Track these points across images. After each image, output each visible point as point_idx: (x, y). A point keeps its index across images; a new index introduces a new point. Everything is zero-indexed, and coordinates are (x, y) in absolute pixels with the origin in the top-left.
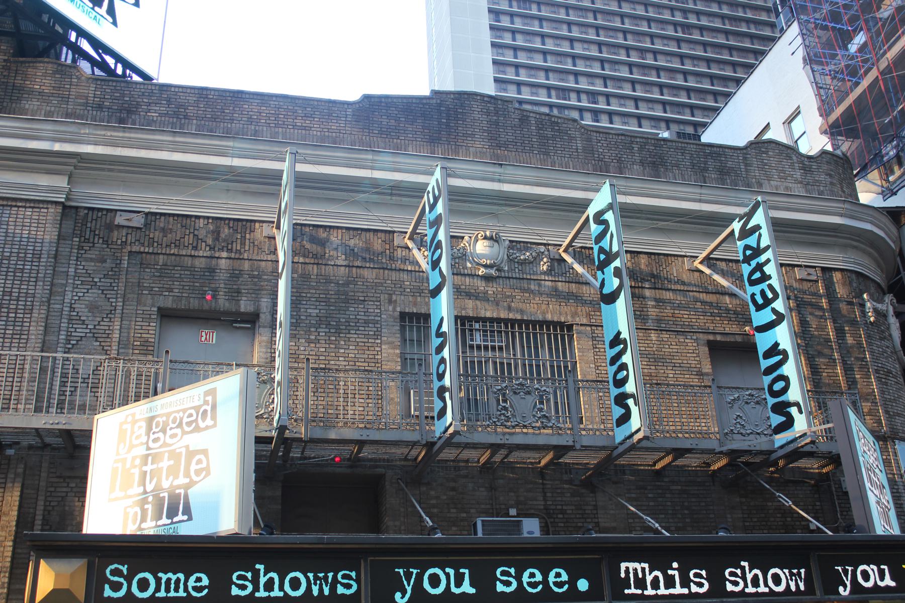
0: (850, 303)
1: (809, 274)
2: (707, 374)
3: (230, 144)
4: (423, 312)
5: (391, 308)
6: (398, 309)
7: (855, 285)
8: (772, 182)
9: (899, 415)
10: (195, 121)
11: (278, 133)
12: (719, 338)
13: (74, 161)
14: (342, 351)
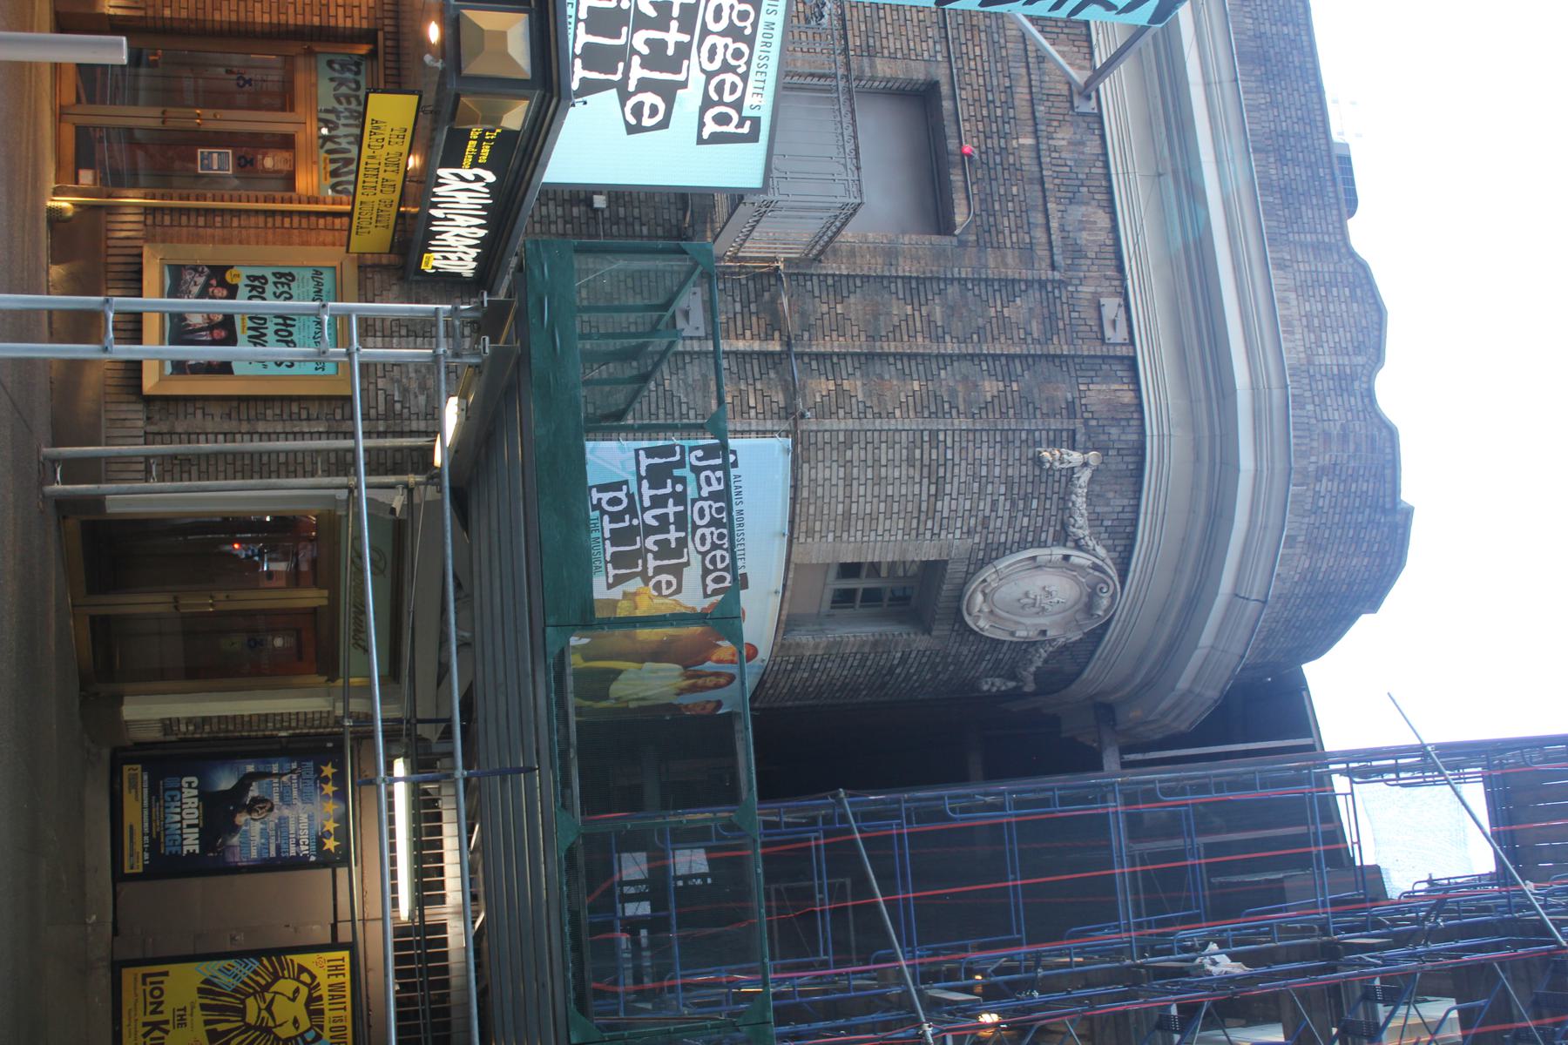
0: (1071, 409)
1: (1114, 322)
2: (872, 66)
7: (1114, 431)
8: (1293, 296)
9: (848, 482)
12: (947, 104)
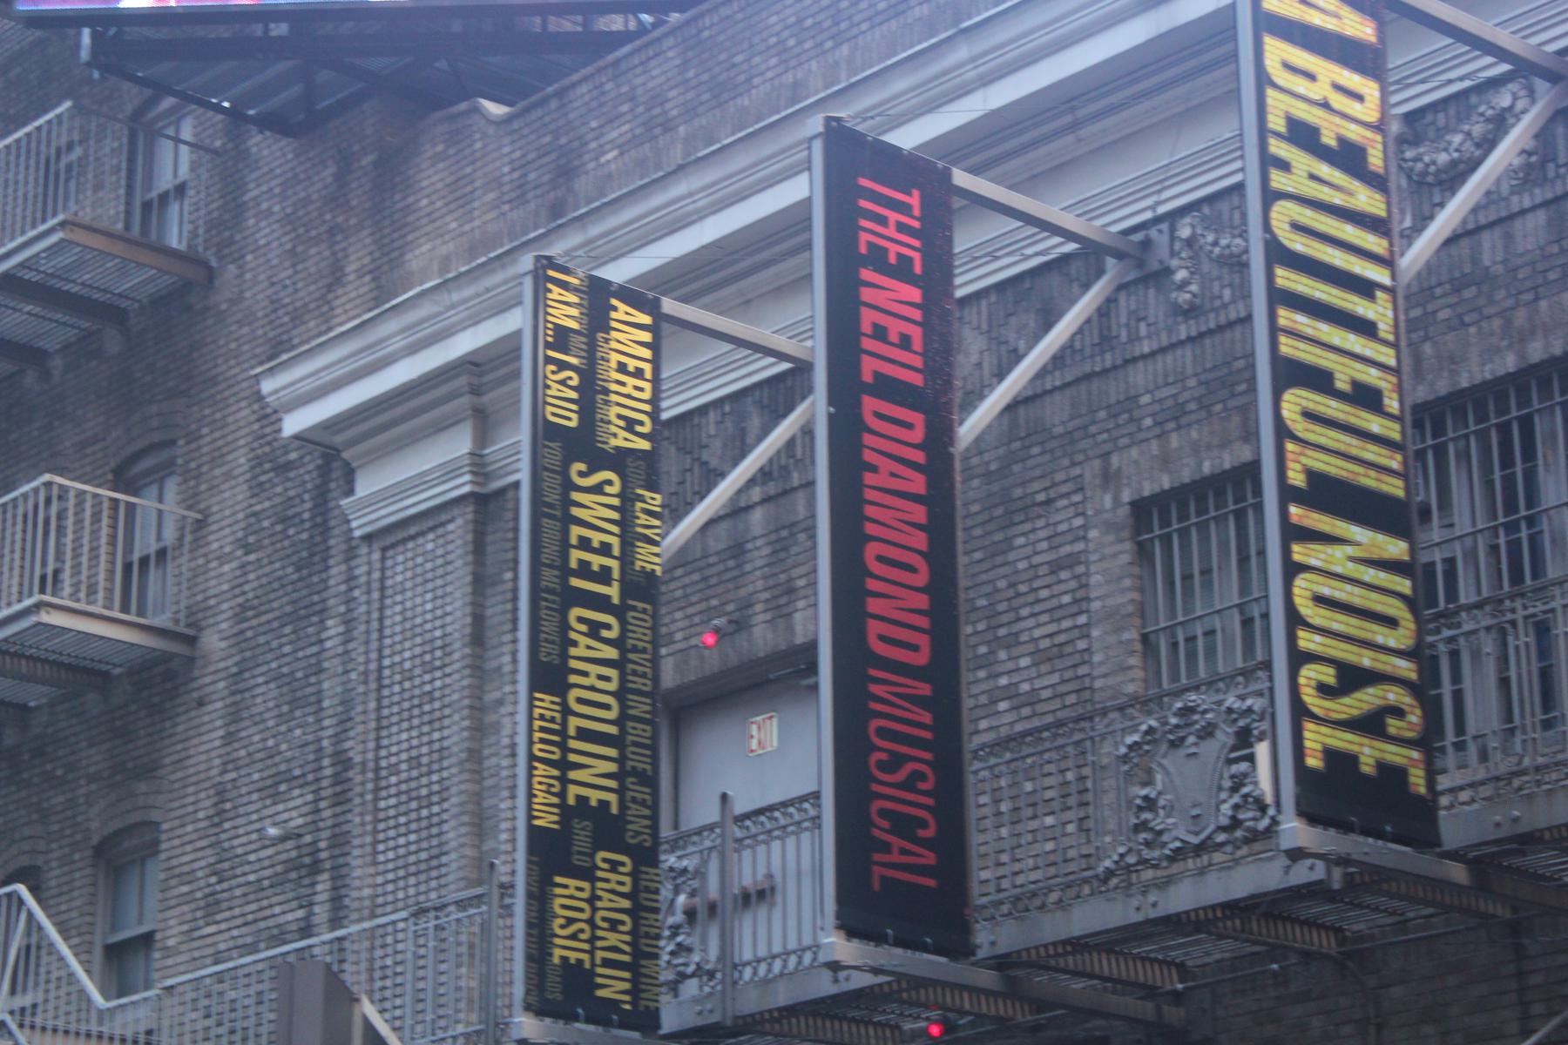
3: (680, 188)
4: (1187, 480)
5: (1108, 501)
6: (1126, 496)
10: (682, 130)
11: (837, 63)
13: (463, 381)
14: (1004, 681)
